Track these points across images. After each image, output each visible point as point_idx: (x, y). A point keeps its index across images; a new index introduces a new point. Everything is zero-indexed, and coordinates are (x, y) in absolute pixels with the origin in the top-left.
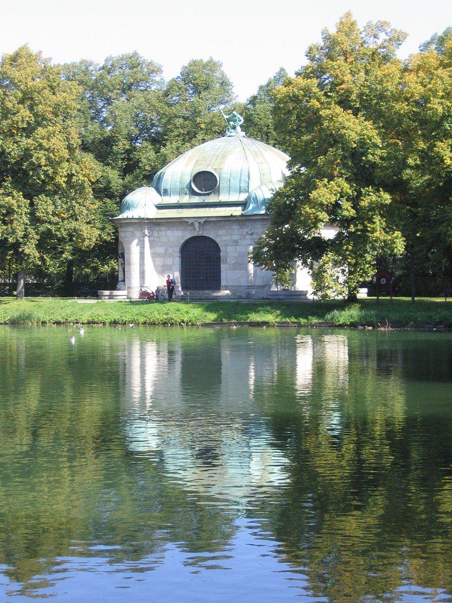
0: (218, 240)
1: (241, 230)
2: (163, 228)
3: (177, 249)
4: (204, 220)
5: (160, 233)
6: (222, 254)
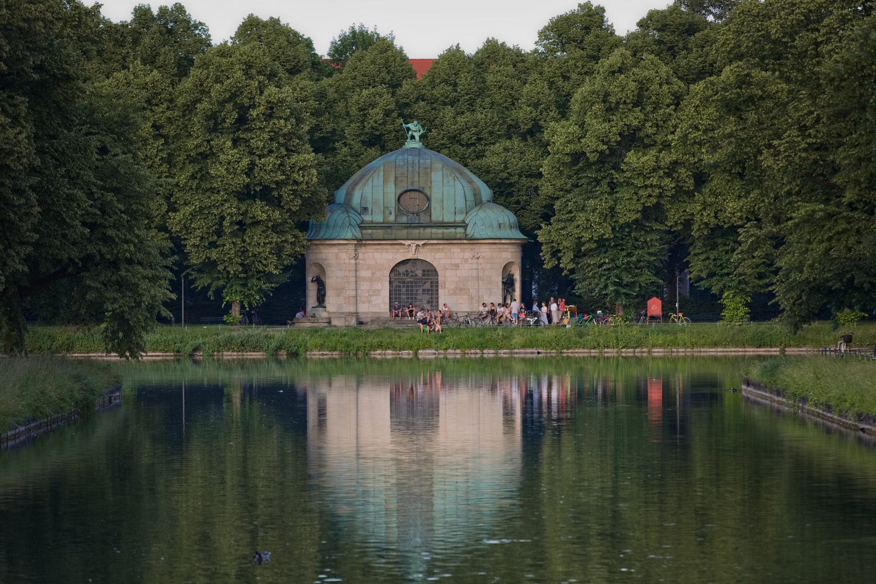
0: (435, 264)
1: (462, 254)
5: (366, 255)
6: (440, 279)
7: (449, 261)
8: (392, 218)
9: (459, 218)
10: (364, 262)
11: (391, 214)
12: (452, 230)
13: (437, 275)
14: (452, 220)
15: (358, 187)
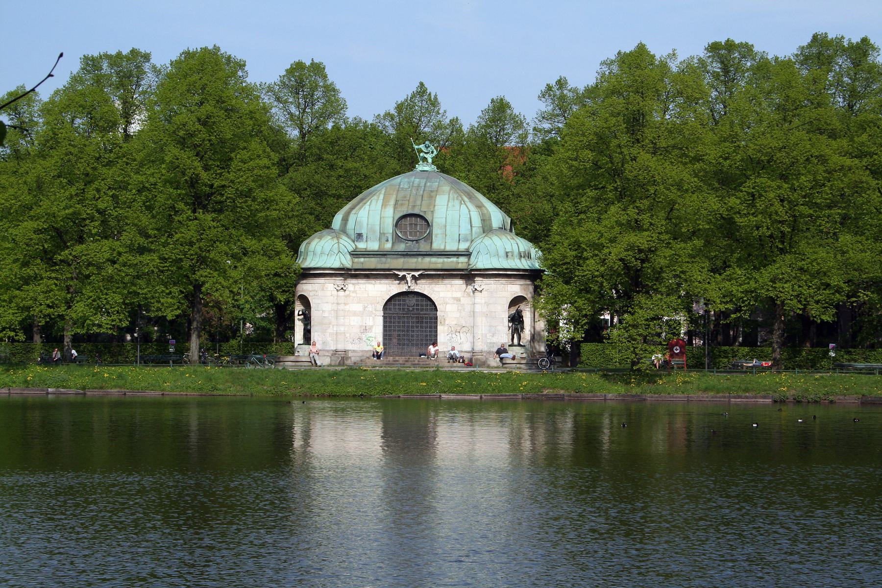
3: (380, 307)
4: (420, 273)
5: (357, 286)
7: (449, 295)
8: (388, 246)
9: (463, 246)
10: (354, 295)
11: (387, 241)
12: (454, 259)
13: (436, 310)
14: (455, 249)
15: (354, 212)
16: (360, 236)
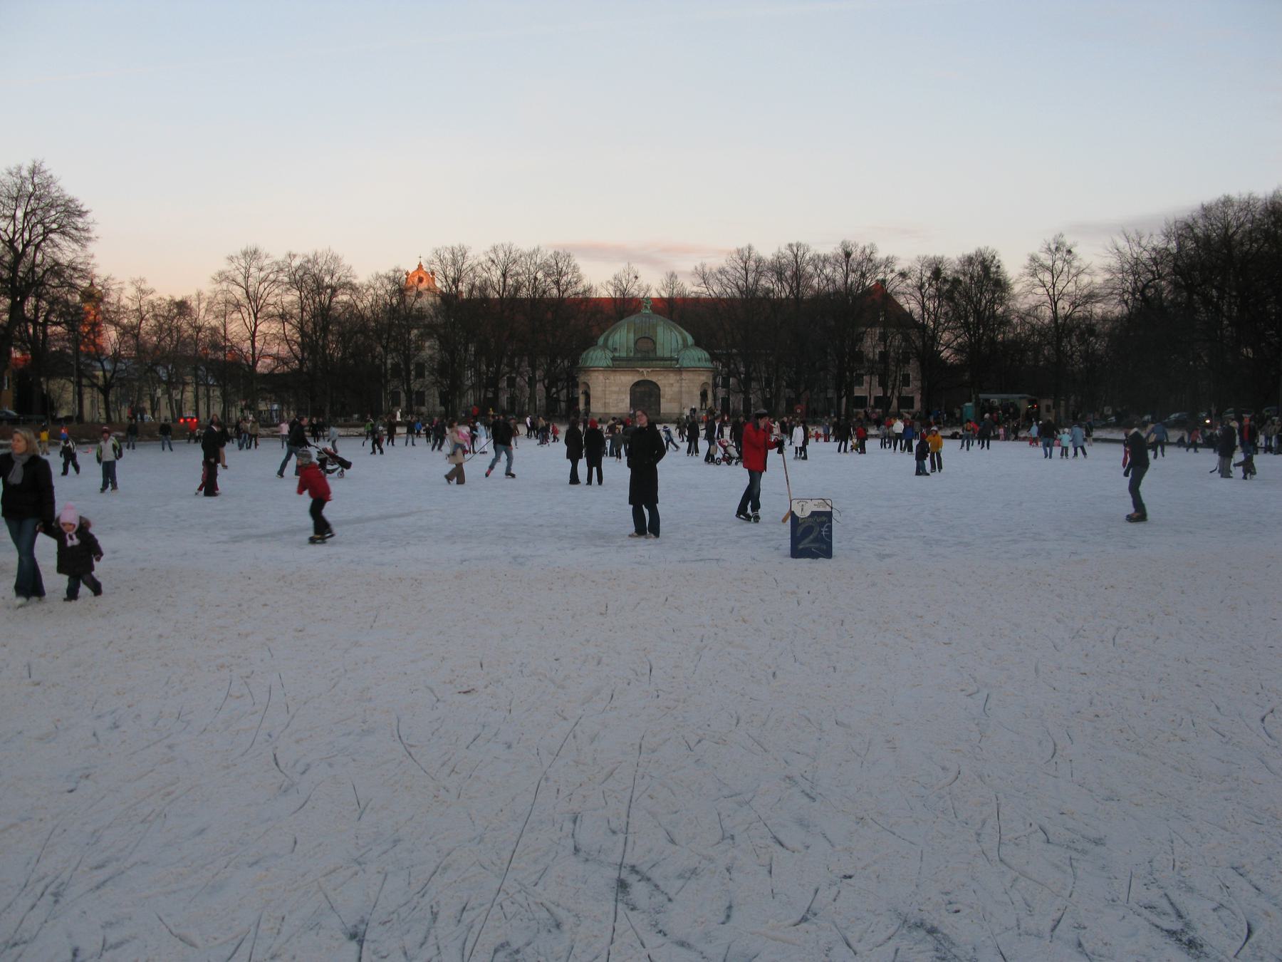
0: (659, 383)
2: (618, 374)
6: (661, 392)
8: (632, 354)
12: (669, 362)
16: (615, 349)
